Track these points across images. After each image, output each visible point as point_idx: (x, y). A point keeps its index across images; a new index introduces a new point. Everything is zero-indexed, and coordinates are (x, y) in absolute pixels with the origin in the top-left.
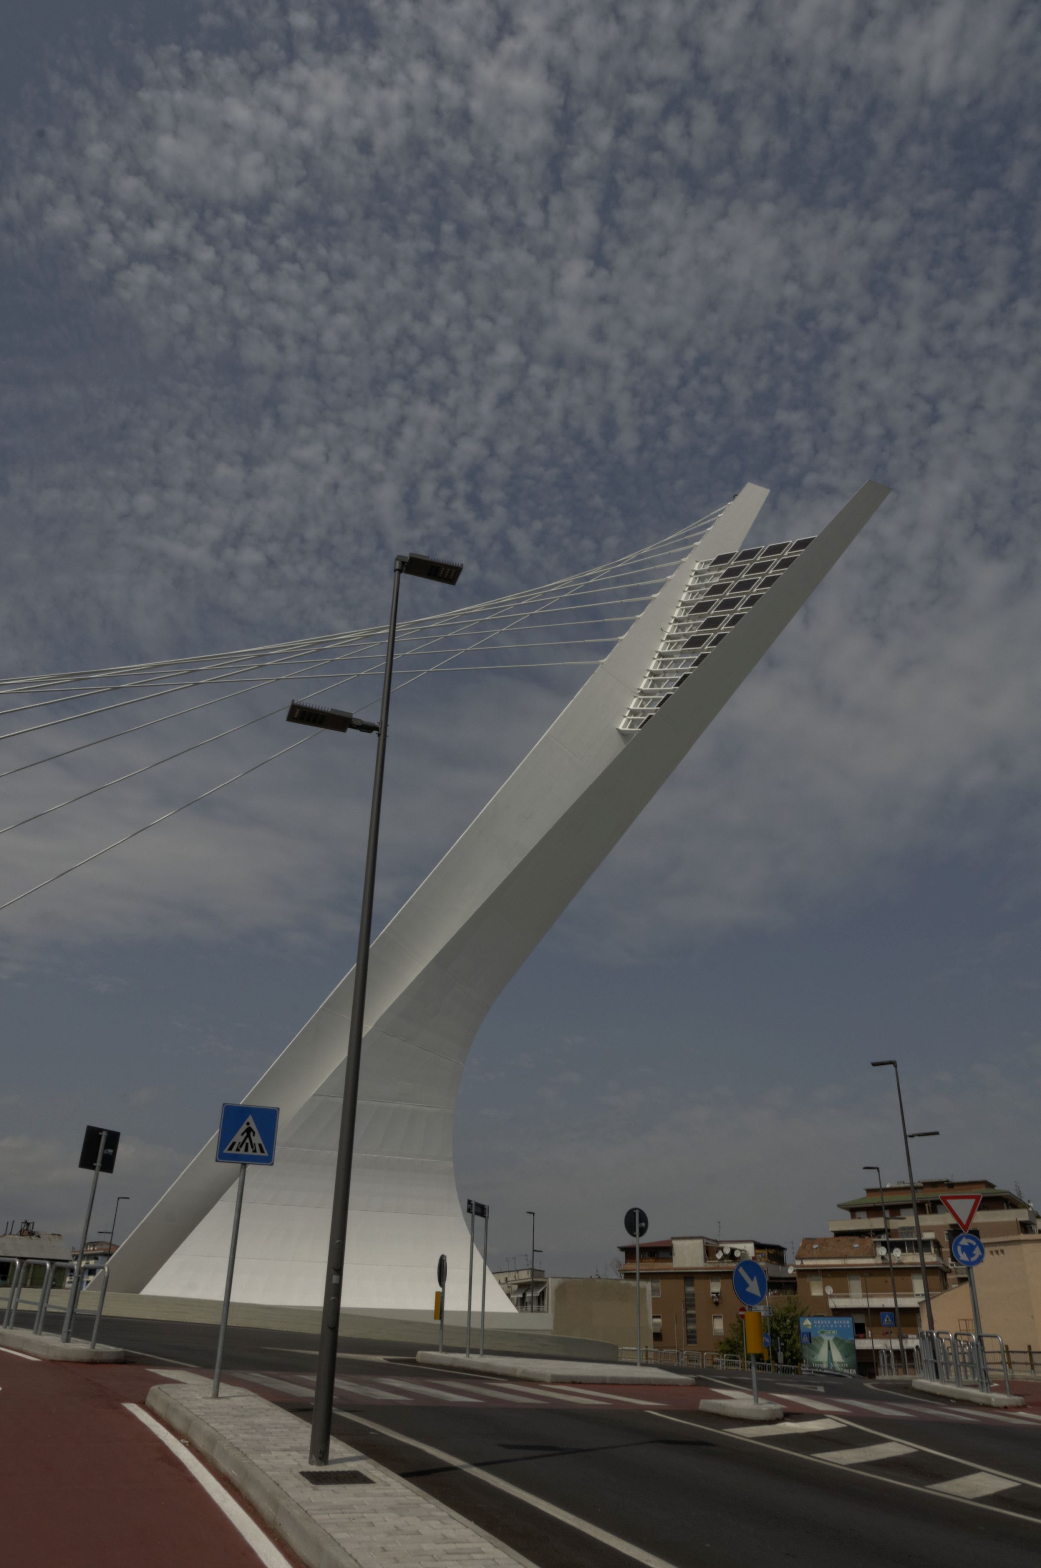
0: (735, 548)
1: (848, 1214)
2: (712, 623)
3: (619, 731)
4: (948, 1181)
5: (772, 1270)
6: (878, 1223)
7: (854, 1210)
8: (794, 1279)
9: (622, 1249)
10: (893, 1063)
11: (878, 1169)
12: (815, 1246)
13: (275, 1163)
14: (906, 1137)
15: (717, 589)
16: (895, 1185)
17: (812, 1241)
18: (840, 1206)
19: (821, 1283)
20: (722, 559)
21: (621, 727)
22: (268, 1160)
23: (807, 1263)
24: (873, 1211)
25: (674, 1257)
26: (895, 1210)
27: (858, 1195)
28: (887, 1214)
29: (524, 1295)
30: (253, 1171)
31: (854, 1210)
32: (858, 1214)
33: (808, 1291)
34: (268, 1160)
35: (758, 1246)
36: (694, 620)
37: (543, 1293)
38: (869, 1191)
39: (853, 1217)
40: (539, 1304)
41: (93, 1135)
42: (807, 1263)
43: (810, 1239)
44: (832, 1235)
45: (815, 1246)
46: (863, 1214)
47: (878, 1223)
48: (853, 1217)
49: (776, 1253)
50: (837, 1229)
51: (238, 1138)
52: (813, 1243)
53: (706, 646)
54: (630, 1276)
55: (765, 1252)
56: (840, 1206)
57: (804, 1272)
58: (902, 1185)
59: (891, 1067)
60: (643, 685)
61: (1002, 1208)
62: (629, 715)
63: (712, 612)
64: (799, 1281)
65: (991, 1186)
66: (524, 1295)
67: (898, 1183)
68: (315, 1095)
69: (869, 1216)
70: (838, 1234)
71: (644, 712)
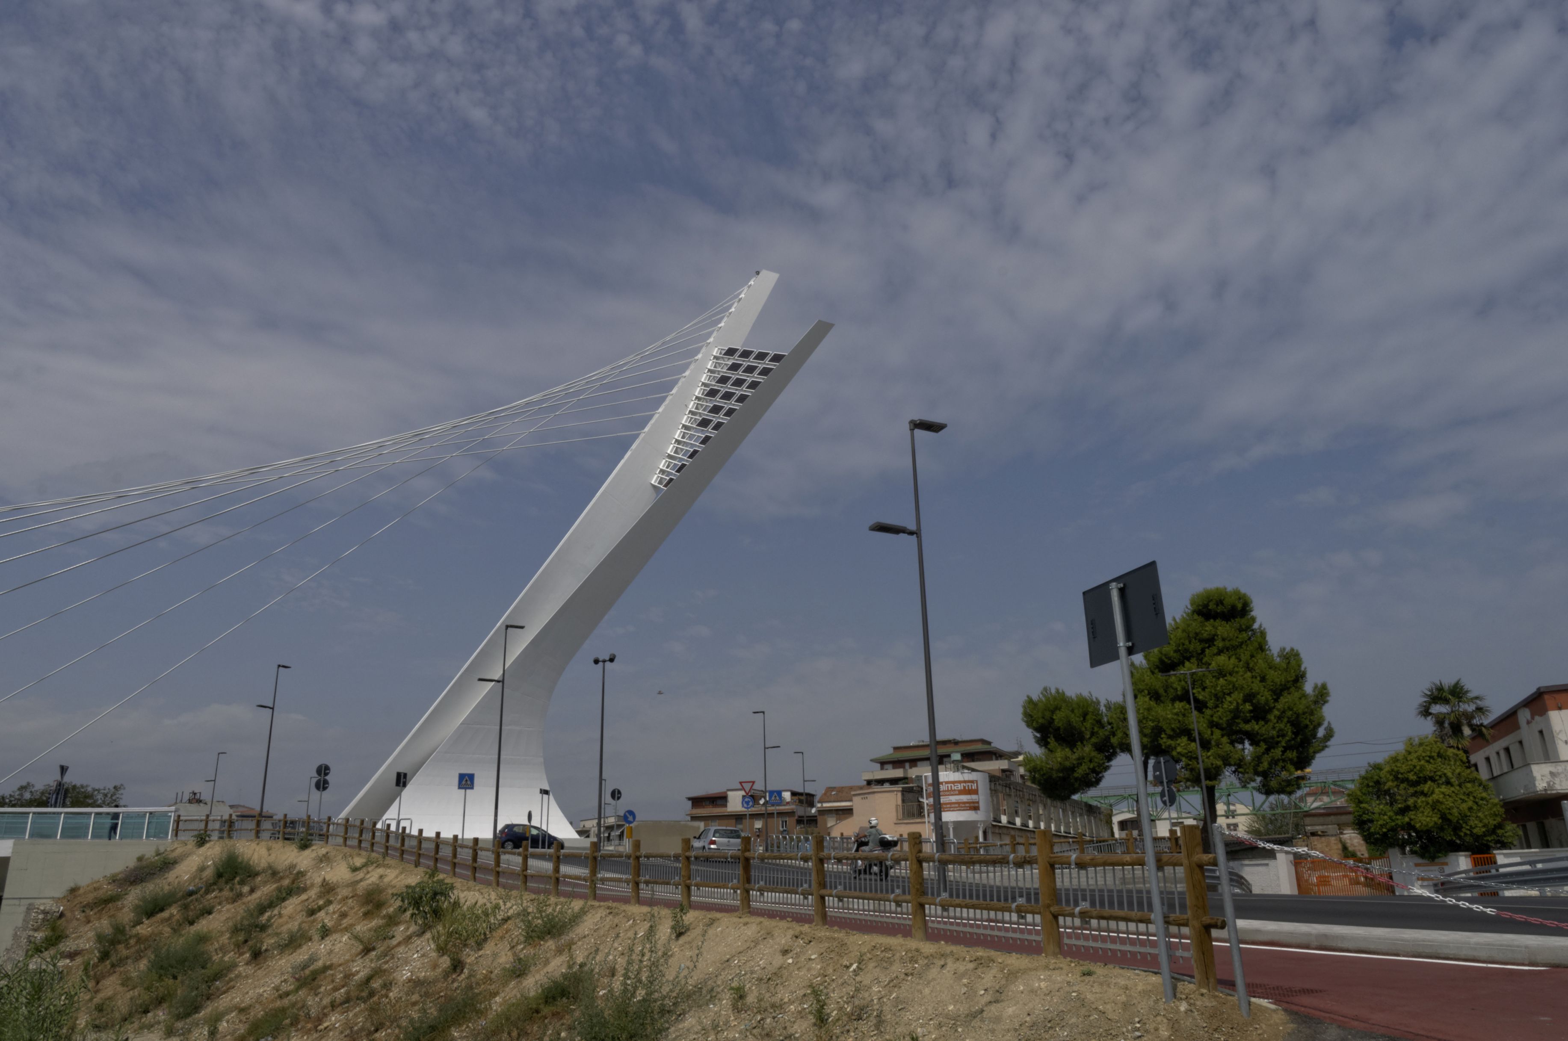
0: (739, 346)
1: (879, 765)
2: (716, 410)
3: (652, 484)
4: (954, 740)
5: (801, 811)
6: (898, 773)
7: (883, 763)
8: (816, 816)
9: (689, 799)
10: (763, 712)
11: (802, 753)
12: (833, 793)
13: (475, 788)
14: (765, 748)
15: (723, 380)
16: (916, 743)
17: (833, 789)
18: (872, 760)
19: (835, 819)
20: (731, 352)
21: (653, 482)
22: (472, 788)
23: (825, 805)
24: (897, 763)
25: (728, 804)
26: (914, 762)
27: (886, 751)
28: (907, 765)
29: (609, 834)
30: (468, 791)
31: (883, 763)
32: (886, 766)
33: (826, 824)
34: (472, 788)
35: (794, 794)
36: (707, 402)
37: (622, 833)
38: (896, 749)
39: (882, 769)
40: (620, 840)
41: (399, 775)
42: (825, 805)
43: (831, 788)
44: (865, 783)
45: (833, 793)
46: (890, 766)
47: (898, 773)
48: (882, 769)
49: (807, 799)
50: (867, 778)
51: (464, 782)
52: (832, 791)
53: (710, 428)
54: (694, 818)
55: (796, 798)
56: (872, 760)
57: (823, 812)
58: (921, 743)
59: (762, 714)
60: (670, 450)
61: (991, 759)
62: (659, 473)
63: (718, 401)
64: (820, 819)
65: (989, 743)
66: (609, 834)
67: (919, 741)
68: (461, 724)
69: (894, 768)
70: (869, 783)
71: (669, 474)
